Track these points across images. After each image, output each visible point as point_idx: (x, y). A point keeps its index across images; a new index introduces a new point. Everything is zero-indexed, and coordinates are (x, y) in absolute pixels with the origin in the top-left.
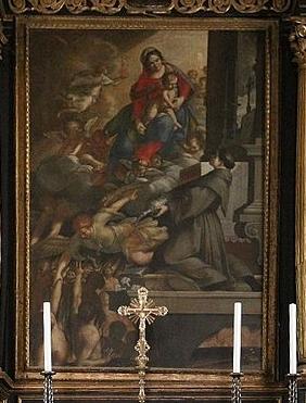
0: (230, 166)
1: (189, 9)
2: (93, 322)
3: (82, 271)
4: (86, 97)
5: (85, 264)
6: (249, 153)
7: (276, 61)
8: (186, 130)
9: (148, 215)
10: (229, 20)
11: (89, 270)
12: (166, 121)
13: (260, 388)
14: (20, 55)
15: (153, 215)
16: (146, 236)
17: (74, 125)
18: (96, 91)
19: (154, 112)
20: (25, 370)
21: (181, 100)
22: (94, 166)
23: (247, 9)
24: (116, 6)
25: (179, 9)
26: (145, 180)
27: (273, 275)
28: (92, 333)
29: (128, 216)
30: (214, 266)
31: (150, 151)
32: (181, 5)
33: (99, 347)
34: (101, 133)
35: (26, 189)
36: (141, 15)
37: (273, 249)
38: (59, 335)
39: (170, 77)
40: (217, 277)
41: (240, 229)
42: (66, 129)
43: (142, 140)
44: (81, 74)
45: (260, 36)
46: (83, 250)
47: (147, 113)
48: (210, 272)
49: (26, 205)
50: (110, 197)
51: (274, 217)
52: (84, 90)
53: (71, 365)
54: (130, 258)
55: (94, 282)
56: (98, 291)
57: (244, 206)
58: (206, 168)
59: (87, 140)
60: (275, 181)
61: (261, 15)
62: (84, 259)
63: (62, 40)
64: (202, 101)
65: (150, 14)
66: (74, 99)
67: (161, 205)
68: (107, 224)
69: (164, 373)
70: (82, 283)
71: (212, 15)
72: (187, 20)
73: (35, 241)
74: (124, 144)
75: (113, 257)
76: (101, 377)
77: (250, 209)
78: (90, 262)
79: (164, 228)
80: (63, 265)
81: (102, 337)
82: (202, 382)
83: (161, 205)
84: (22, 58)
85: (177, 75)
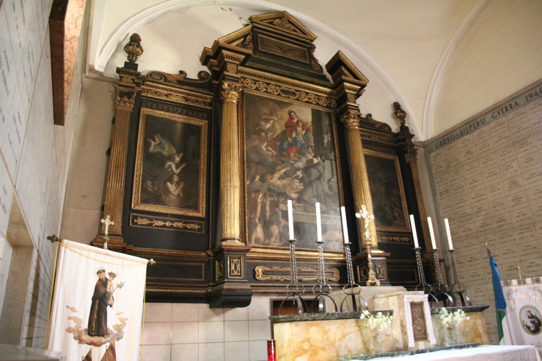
0: (324, 162)
2: (275, 224)
3: (269, 199)
5: (271, 196)
6: (330, 158)
9: (295, 177)
11: (272, 199)
12: (299, 139)
15: (297, 177)
16: (295, 186)
17: (263, 134)
18: (272, 122)
19: (294, 135)
21: (304, 132)
29: (287, 176)
33: (278, 237)
34: (274, 139)
42: (260, 135)
43: (290, 145)
44: (266, 114)
47: (292, 135)
52: (267, 121)
53: (267, 245)
56: (277, 210)
57: (331, 178)
58: (315, 161)
64: (311, 134)
65: (289, 98)
68: (279, 179)
77: (332, 180)
78: (272, 195)
79: (302, 184)
80: (261, 196)
81: (280, 232)
83: (299, 174)
85: (302, 122)
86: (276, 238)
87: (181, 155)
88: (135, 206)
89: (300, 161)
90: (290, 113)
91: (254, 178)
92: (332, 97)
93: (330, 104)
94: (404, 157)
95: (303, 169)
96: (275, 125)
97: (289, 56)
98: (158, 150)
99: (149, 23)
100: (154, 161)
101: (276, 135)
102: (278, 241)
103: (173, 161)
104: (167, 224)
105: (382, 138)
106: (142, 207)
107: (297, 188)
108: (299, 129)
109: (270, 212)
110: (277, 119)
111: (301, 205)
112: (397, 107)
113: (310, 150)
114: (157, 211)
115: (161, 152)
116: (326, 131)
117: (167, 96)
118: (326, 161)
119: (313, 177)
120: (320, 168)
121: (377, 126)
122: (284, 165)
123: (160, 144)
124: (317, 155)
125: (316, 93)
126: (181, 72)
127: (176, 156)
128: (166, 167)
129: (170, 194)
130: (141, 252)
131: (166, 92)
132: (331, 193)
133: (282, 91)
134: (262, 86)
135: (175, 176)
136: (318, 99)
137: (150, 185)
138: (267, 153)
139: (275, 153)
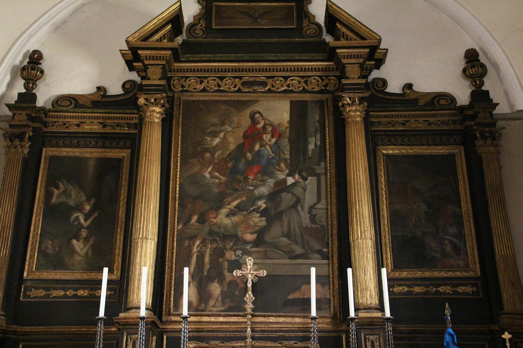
0: (305, 179)
1: (278, 88)
2: (216, 280)
3: (210, 246)
4: (215, 139)
6: (317, 172)
7: (331, 117)
8: (277, 157)
9: (254, 210)
10: (301, 95)
11: (215, 245)
12: (265, 152)
13: (329, 327)
14: (176, 114)
15: (256, 210)
16: (252, 223)
17: (208, 155)
18: (222, 135)
19: (257, 147)
20: (169, 314)
21: (274, 140)
22: (220, 180)
23: (313, 88)
24: (235, 87)
25: (273, 89)
26: (252, 188)
27: (335, 249)
28: (216, 289)
29: (240, 210)
30: (297, 243)
31: (255, 170)
32: (273, 86)
33: (220, 298)
34: (225, 161)
35: (176, 194)
36: (250, 92)
37: (335, 232)
38: (194, 290)
39: (267, 127)
40: (299, 250)
41: (313, 218)
42: (203, 158)
43: (249, 164)
44: (213, 125)
45: (321, 104)
46: (211, 233)
47: (253, 147)
48: (294, 247)
49: (175, 204)
50: (229, 199)
51: (334, 211)
52: (215, 134)
53: (201, 311)
54: (242, 238)
55: (218, 253)
56: (221, 260)
57: (315, 204)
58: (290, 181)
59: (216, 164)
60: (334, 189)
61: (321, 92)
62: (211, 238)
63: (202, 106)
64: (287, 140)
65: (255, 92)
66: (209, 139)
67: (262, 204)
68: (227, 216)
69: (264, 316)
70: (210, 254)
71: (292, 92)
72: (277, 95)
73: (180, 226)
74: (238, 167)
75: (231, 237)
76: (221, 319)
77: (319, 206)
78: (216, 240)
79: (264, 218)
80: (198, 243)
81: (222, 291)
82: (290, 323)
83: (262, 204)
84: (178, 116)
85: (271, 125)
86: (217, 300)
87: (93, 201)
88: (28, 274)
89: (264, 185)
90: (252, 117)
91: (190, 219)
92: (330, 74)
93: (326, 86)
94: (475, 145)
95: (267, 196)
96: (227, 138)
97: (265, 24)
98: (63, 199)
99: (57, 28)
100: (56, 214)
101: (228, 152)
102: (219, 304)
103: (81, 211)
104: (68, 293)
105: (431, 120)
106: (37, 275)
107: (255, 226)
108: (266, 137)
109: (210, 264)
110: (230, 129)
111: (261, 249)
112: (472, 57)
113: (283, 166)
114: (57, 277)
115: (65, 203)
116: (313, 130)
117: (78, 125)
118: (310, 178)
119: (283, 206)
120: (298, 190)
121: (422, 103)
122: (238, 194)
123: (64, 192)
124: (295, 172)
125: (302, 74)
126: (99, 88)
127: (86, 204)
128: (72, 219)
129: (75, 255)
130: (31, 332)
131: (76, 121)
132: (314, 226)
133: (243, 84)
134: (212, 84)
135: (83, 230)
136: (306, 82)
137: (49, 246)
138: (213, 180)
139: (223, 179)
